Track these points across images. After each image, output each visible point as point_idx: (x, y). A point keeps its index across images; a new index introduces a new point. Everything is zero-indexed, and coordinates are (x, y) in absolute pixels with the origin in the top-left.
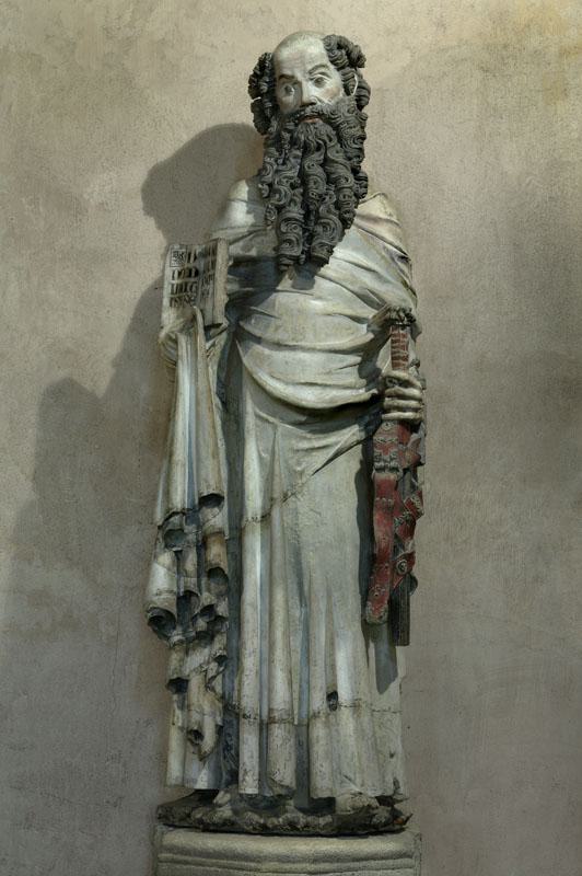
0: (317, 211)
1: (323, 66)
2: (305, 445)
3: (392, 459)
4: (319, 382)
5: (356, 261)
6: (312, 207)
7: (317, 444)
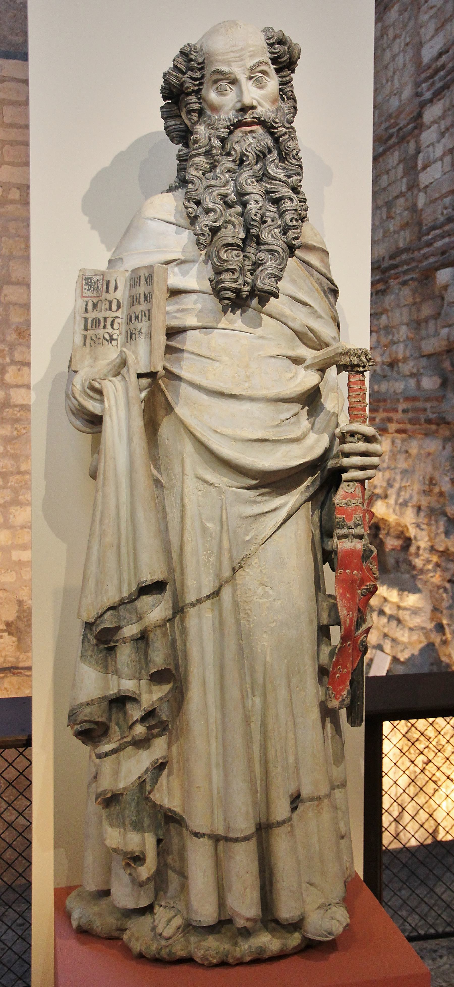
0: (258, 237)
1: (266, 63)
3: (356, 526)
5: (293, 294)
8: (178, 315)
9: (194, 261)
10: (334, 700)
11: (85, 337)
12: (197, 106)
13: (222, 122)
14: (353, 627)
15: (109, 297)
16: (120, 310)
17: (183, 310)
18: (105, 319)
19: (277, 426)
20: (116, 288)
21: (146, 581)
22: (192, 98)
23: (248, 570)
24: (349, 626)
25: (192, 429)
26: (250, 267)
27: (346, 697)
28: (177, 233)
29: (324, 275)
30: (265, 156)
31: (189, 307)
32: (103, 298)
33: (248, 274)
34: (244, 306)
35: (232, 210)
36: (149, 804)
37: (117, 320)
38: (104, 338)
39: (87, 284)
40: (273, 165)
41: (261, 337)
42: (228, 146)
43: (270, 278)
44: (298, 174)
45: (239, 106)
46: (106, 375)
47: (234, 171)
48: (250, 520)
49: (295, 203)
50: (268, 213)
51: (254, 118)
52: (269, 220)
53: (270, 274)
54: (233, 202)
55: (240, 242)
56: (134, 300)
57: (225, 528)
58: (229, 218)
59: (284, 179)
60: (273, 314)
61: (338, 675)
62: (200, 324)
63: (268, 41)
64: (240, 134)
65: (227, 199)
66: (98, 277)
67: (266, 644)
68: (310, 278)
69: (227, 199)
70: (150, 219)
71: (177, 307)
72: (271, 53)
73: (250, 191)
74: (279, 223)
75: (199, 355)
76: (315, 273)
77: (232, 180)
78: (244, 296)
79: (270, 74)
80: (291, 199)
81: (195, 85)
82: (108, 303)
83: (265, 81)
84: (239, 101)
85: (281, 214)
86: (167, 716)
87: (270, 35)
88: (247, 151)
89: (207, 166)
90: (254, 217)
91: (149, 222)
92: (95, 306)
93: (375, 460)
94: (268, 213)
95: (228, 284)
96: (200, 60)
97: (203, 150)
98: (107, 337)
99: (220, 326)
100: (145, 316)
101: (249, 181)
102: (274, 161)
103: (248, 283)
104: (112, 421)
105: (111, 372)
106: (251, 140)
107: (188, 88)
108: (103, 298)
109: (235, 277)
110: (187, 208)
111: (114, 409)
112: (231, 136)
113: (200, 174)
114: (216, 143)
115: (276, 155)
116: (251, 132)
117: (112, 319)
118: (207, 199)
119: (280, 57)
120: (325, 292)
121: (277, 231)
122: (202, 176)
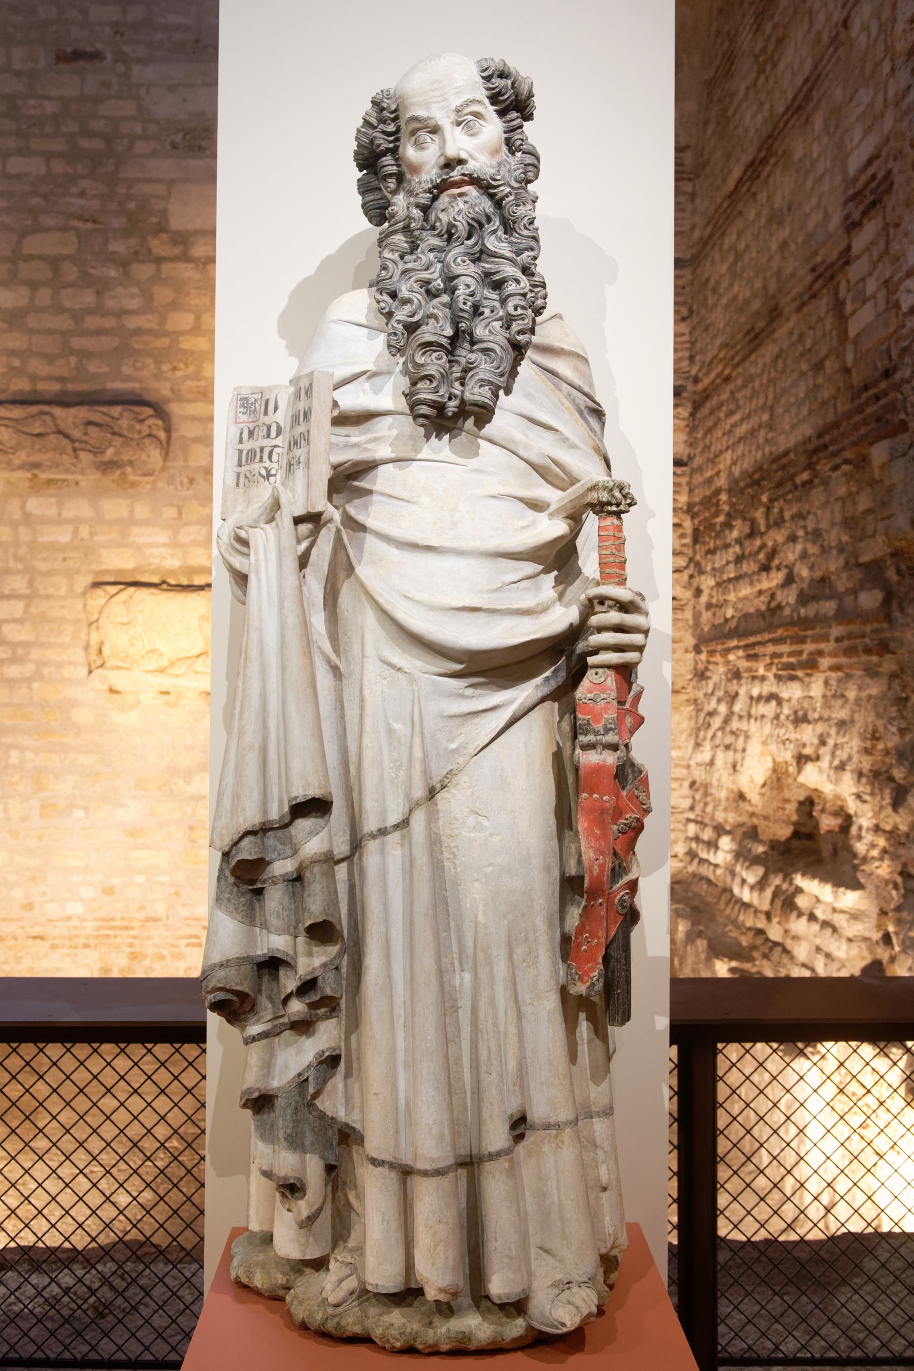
0: (471, 334)
3: (607, 730)
4: (485, 605)
6: (463, 325)
8: (369, 446)
9: (389, 373)
10: (579, 984)
11: (238, 475)
12: (394, 169)
13: (423, 185)
15: (268, 420)
16: (281, 437)
17: (376, 439)
18: (262, 449)
19: (497, 590)
20: (276, 408)
21: (296, 797)
22: (388, 160)
23: (455, 792)
24: (598, 876)
25: (373, 594)
26: (459, 375)
28: (370, 338)
29: (579, 389)
30: (481, 226)
31: (382, 434)
32: (260, 423)
33: (457, 384)
34: (454, 429)
35: (436, 301)
36: (314, 1113)
37: (276, 450)
38: (260, 474)
39: (242, 406)
40: (493, 238)
41: (478, 471)
42: (432, 217)
43: (481, 386)
44: (532, 249)
45: (442, 161)
46: (256, 521)
47: (441, 250)
48: (456, 722)
49: (522, 285)
50: (486, 302)
51: (464, 175)
52: (487, 312)
53: (482, 380)
54: (438, 290)
55: (445, 342)
56: (295, 420)
57: (417, 730)
58: (431, 310)
59: (509, 255)
60: (496, 440)
62: (393, 455)
63: (484, 74)
64: (447, 199)
65: (430, 286)
66: (256, 396)
67: (477, 896)
68: (557, 392)
69: (430, 286)
70: (335, 322)
71: (369, 436)
72: (488, 89)
73: (459, 272)
74: (501, 313)
75: (391, 496)
76: (565, 385)
77: (439, 262)
78: (450, 414)
79: (487, 116)
80: (517, 281)
81: (390, 142)
82: (265, 428)
83: (478, 126)
84: (442, 154)
85: (503, 301)
86: (332, 989)
87: (485, 66)
88: (455, 220)
89: (406, 246)
90: (461, 306)
91: (333, 326)
92: (251, 433)
93: (637, 638)
94: (486, 302)
95: (422, 396)
96: (393, 107)
97: (401, 225)
99: (419, 456)
101: (459, 260)
102: (495, 232)
103: (456, 396)
104: (259, 580)
105: (263, 517)
106: (461, 205)
107: (379, 145)
108: (260, 423)
109: (434, 385)
110: (378, 302)
111: (263, 564)
112: (436, 203)
113: (396, 256)
114: (416, 213)
115: (497, 223)
116: (461, 195)
118: (404, 288)
119: (499, 94)
120: (581, 412)
121: (497, 324)
122: (398, 259)
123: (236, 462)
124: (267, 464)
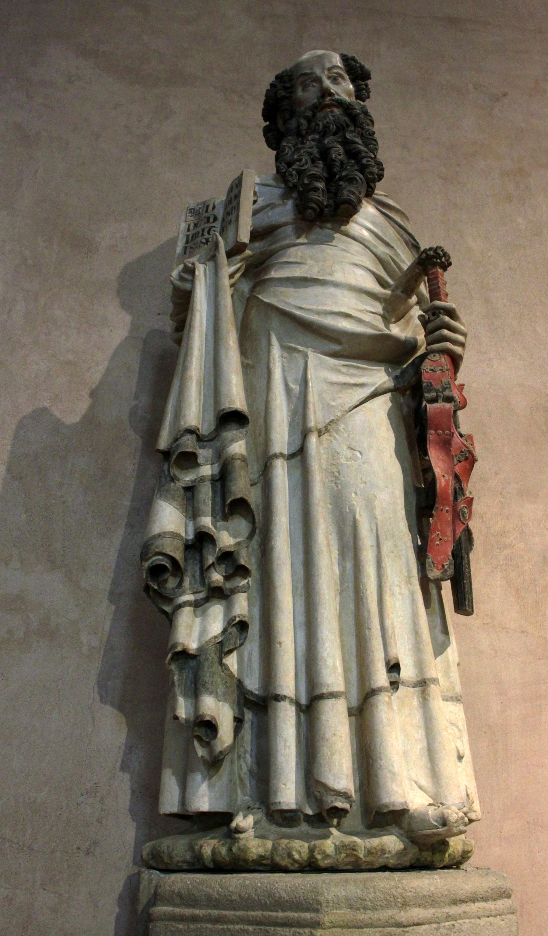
2: (343, 379)
7: (352, 381)
10: (435, 570)
14: (450, 491)
16: (216, 223)
23: (336, 435)
24: (445, 486)
27: (449, 567)
38: (201, 242)
39: (190, 212)
61: (438, 542)
86: (245, 561)
93: (461, 338)
98: (204, 241)
100: (235, 209)
117: (208, 229)
123: (184, 241)
124: (206, 236)
